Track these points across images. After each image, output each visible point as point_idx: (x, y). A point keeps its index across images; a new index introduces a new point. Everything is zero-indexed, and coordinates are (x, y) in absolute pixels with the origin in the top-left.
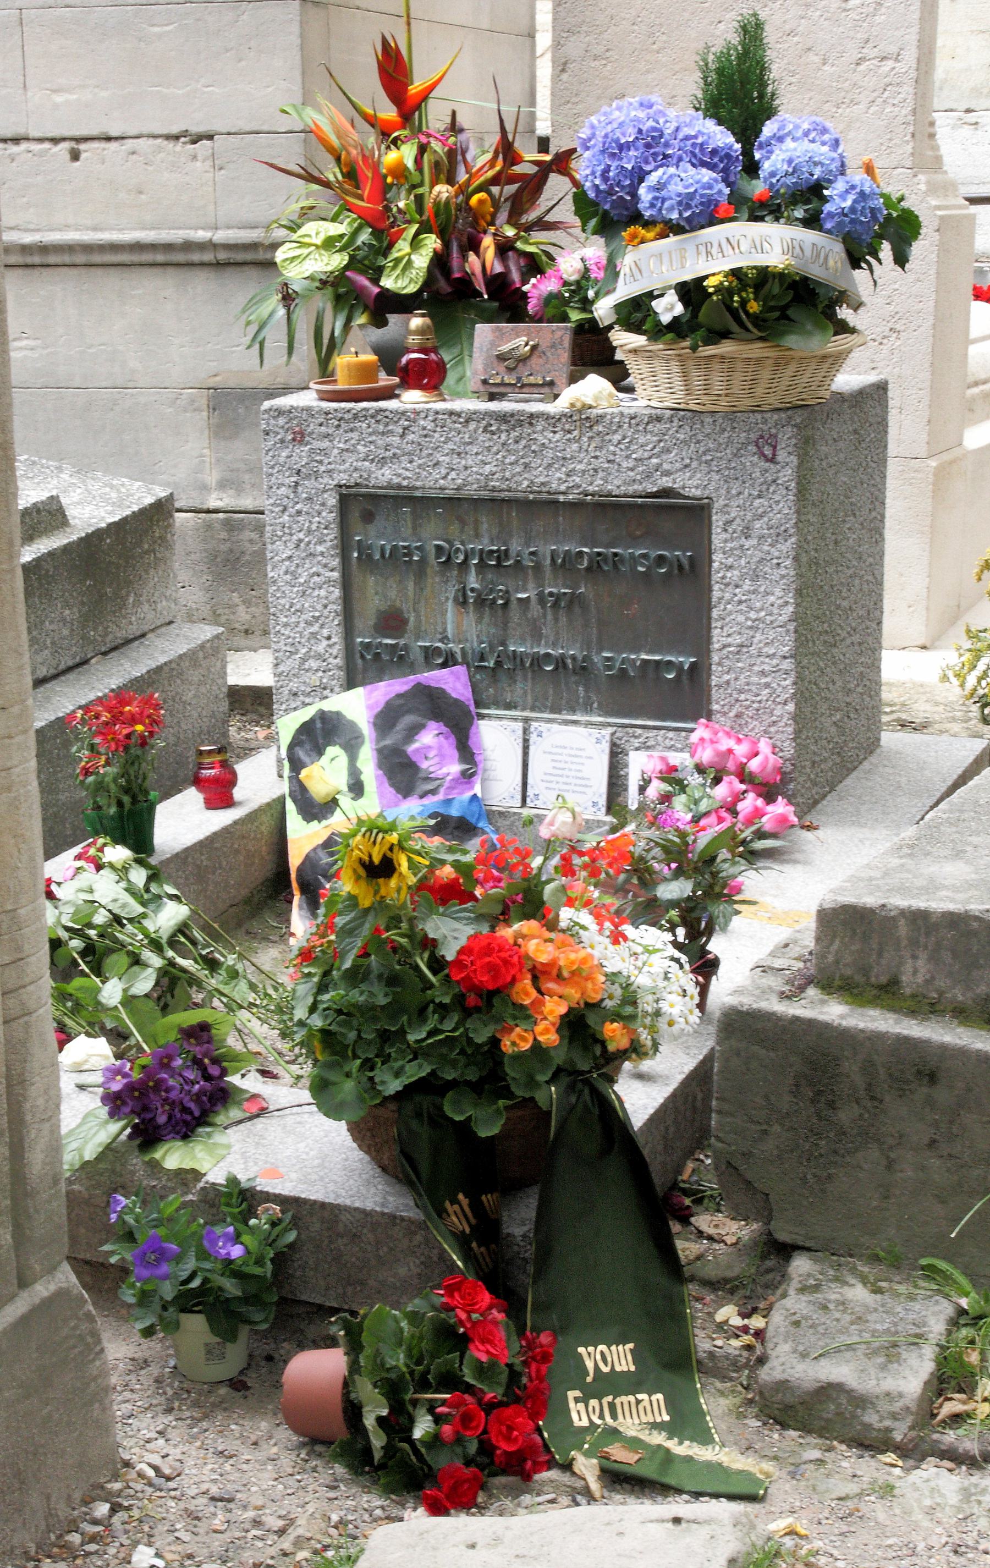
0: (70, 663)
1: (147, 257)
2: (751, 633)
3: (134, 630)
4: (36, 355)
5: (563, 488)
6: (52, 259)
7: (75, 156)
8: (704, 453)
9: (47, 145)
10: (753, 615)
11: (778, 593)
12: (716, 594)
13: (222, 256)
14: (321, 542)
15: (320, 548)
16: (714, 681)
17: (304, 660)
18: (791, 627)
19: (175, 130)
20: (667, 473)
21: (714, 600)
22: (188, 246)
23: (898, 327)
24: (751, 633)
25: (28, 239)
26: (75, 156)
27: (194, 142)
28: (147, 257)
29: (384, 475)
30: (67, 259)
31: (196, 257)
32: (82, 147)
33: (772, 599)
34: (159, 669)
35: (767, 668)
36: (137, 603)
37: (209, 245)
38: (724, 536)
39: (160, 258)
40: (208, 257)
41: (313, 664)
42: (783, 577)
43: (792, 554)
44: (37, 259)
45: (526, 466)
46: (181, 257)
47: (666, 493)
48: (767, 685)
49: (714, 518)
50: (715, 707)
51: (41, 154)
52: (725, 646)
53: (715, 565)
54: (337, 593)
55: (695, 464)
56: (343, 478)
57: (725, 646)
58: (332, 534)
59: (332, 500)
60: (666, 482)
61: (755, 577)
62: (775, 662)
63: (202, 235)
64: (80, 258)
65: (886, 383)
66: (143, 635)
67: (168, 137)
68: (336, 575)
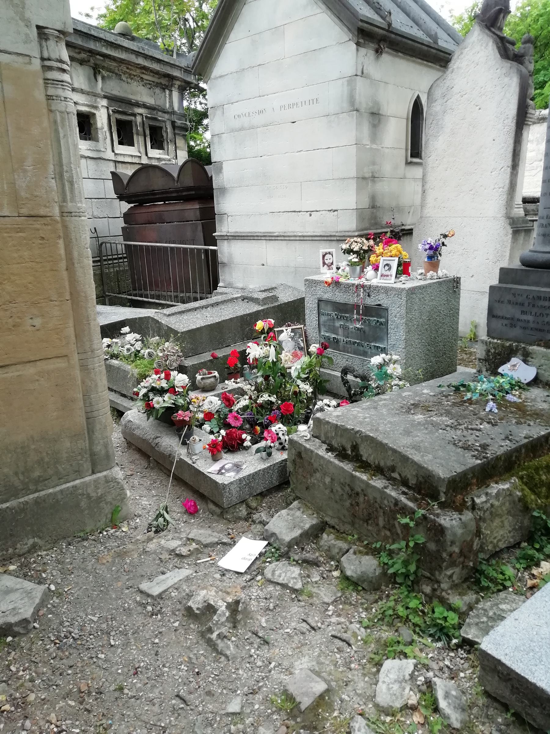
1: (323, 238)
6: (305, 238)
7: (311, 215)
13: (338, 238)
22: (331, 236)
25: (300, 234)
26: (311, 215)
28: (323, 238)
29: (326, 296)
30: (308, 238)
31: (332, 238)
37: (335, 236)
39: (325, 238)
40: (335, 239)
44: (302, 238)
46: (329, 238)
56: (318, 296)
58: (316, 308)
60: (379, 303)
61: (397, 328)
63: (334, 234)
64: (311, 239)
65: (460, 278)
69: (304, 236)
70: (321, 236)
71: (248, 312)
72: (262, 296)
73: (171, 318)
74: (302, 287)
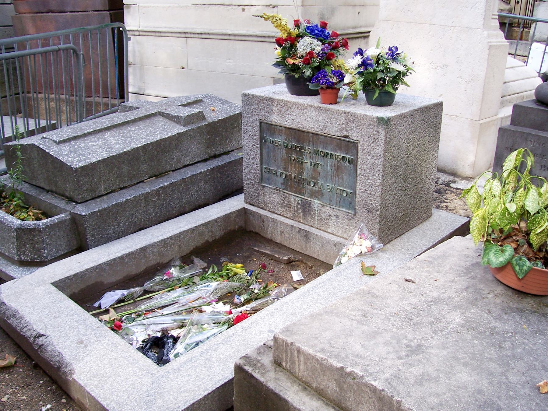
0: (200, 160)
2: (368, 187)
3: (229, 149)
4: (231, 64)
5: (318, 130)
7: (243, 10)
8: (357, 126)
9: (237, 7)
10: (369, 181)
11: (377, 175)
12: (359, 172)
14: (255, 136)
15: (255, 137)
16: (357, 199)
17: (251, 170)
18: (380, 187)
19: (268, 4)
20: (346, 131)
21: (358, 174)
23: (474, 79)
24: (368, 187)
26: (243, 10)
27: (274, 7)
32: (246, 7)
33: (375, 177)
34: (231, 162)
35: (372, 199)
36: (231, 141)
38: (362, 154)
41: (253, 171)
42: (379, 170)
43: (382, 163)
44: (232, 38)
45: (308, 121)
47: (345, 137)
48: (372, 204)
49: (359, 147)
50: (357, 208)
51: (234, 9)
52: (360, 189)
53: (359, 163)
54: (259, 151)
55: (355, 129)
57: (360, 189)
59: (258, 124)
60: (346, 133)
62: (375, 197)
66: (233, 150)
67: (267, 6)
68: (259, 146)
69: (235, 35)
70: (257, 36)
71: (166, 135)
72: (186, 112)
73: (62, 146)
74: (238, 102)
